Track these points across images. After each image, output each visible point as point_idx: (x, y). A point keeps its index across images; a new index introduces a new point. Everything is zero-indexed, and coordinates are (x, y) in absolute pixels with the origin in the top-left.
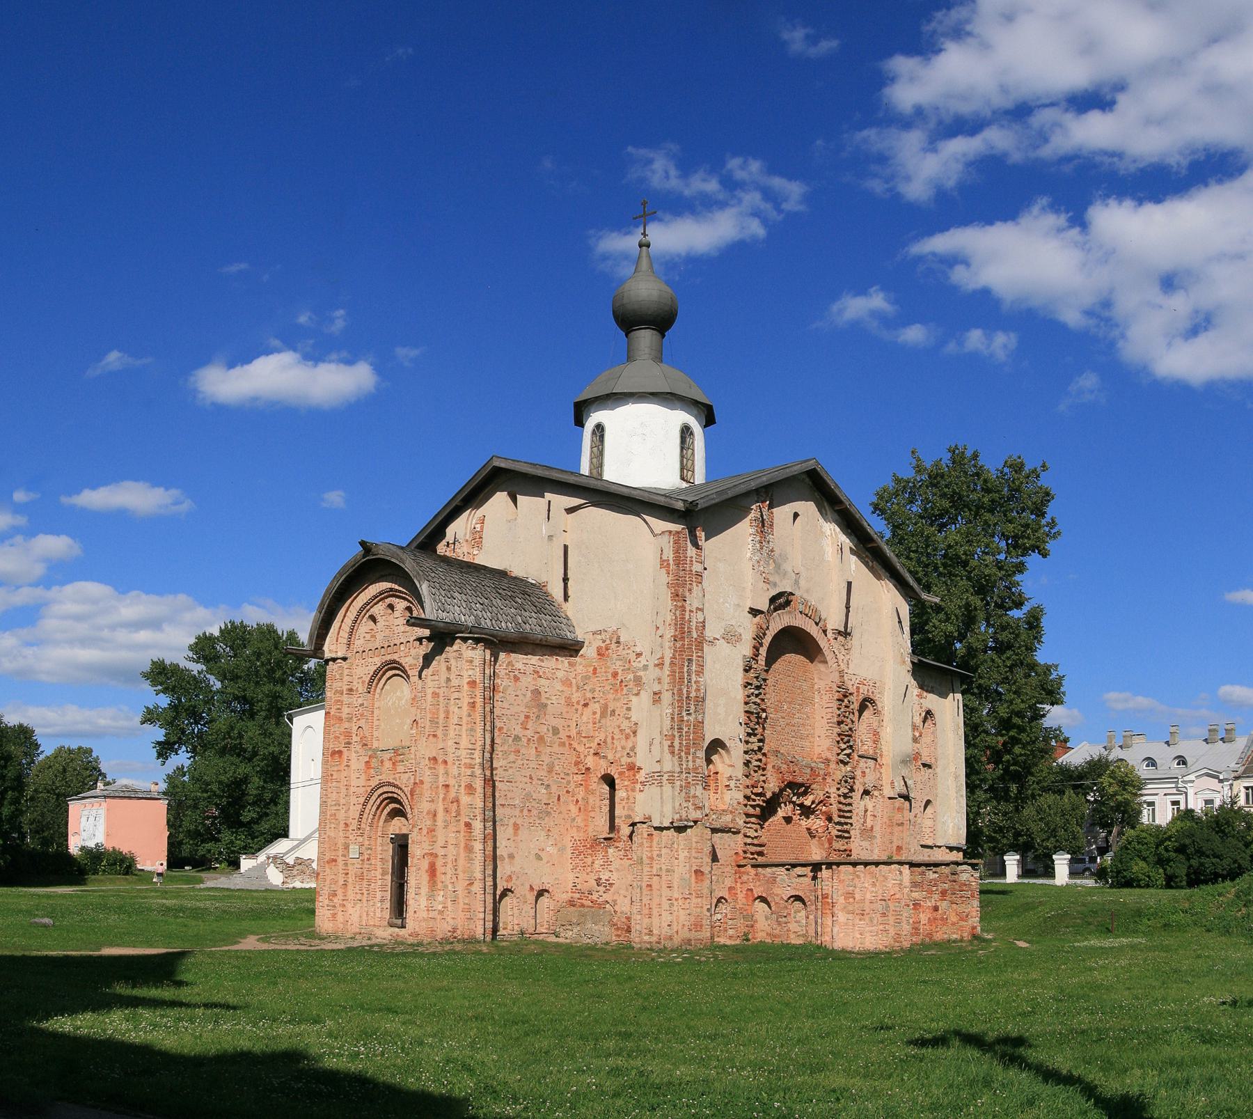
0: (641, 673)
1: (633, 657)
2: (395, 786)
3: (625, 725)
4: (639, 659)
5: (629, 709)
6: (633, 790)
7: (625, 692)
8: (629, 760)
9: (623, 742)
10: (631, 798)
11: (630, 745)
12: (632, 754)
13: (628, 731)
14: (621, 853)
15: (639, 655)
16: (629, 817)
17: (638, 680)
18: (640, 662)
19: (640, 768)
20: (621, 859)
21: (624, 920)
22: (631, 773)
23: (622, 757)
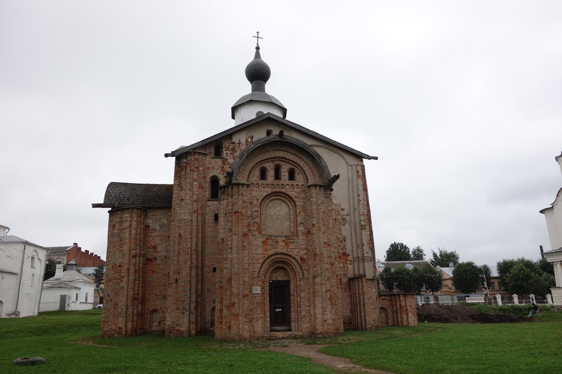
0: (345, 217)
1: (340, 210)
2: (289, 255)
3: (339, 236)
4: (343, 211)
5: (340, 230)
6: (346, 264)
7: (338, 223)
8: (343, 251)
9: (339, 244)
10: (346, 268)
11: (343, 245)
12: (344, 249)
13: (341, 239)
14: (343, 290)
15: (343, 209)
16: (345, 275)
17: (344, 220)
18: (344, 212)
19: (348, 255)
20: (343, 293)
21: (347, 319)
22: (345, 256)
23: (340, 250)
